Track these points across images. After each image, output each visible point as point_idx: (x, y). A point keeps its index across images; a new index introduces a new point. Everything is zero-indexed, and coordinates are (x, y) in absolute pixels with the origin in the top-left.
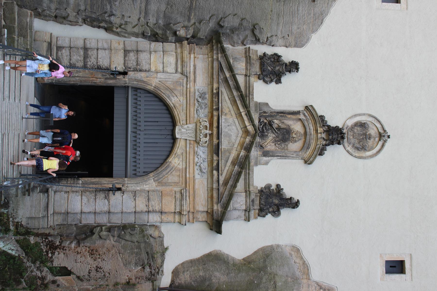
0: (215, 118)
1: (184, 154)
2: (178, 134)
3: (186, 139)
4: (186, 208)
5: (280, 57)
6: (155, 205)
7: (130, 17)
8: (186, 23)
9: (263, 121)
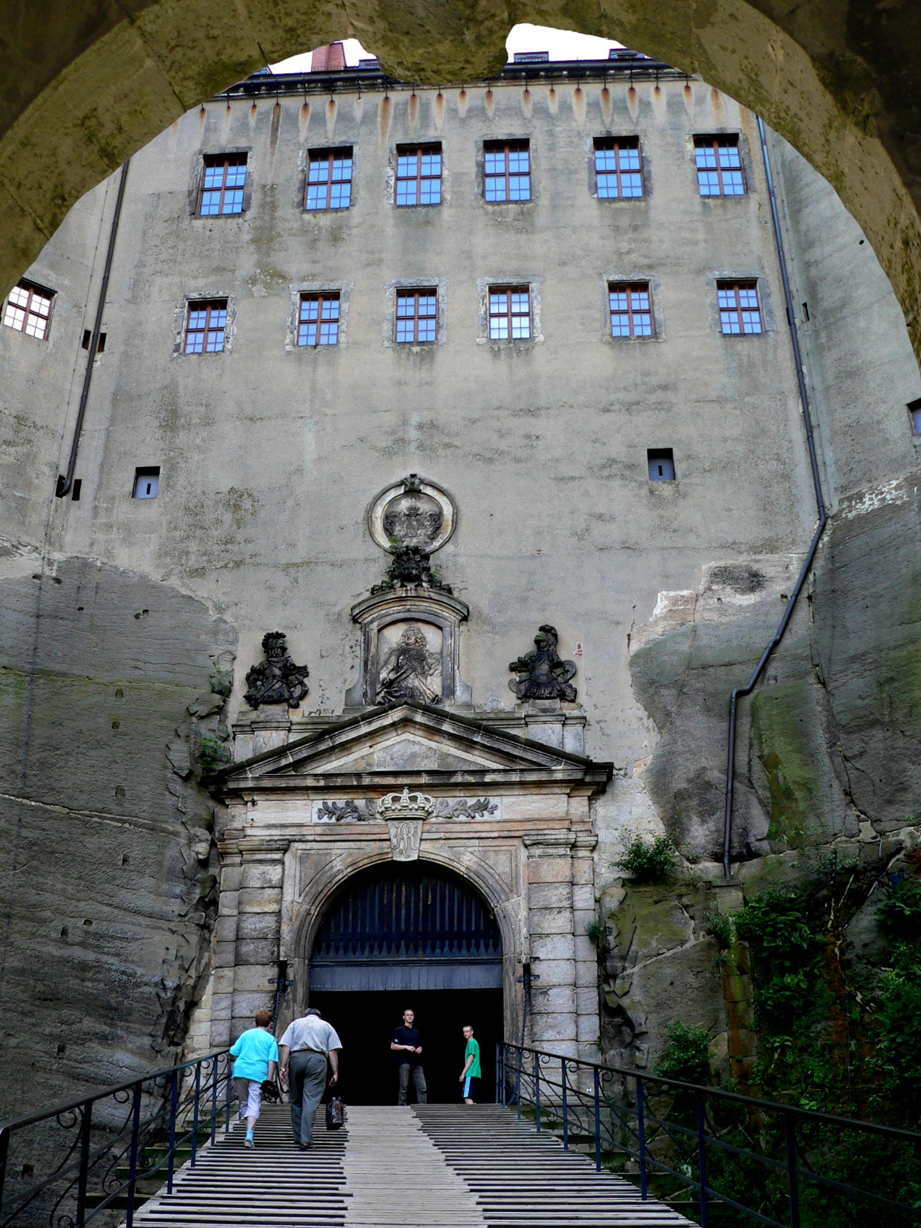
0: (378, 780)
1: (451, 842)
2: (409, 856)
3: (421, 840)
4: (562, 835)
5: (253, 670)
6: (556, 896)
7: (167, 949)
8: (183, 841)
9: (383, 698)
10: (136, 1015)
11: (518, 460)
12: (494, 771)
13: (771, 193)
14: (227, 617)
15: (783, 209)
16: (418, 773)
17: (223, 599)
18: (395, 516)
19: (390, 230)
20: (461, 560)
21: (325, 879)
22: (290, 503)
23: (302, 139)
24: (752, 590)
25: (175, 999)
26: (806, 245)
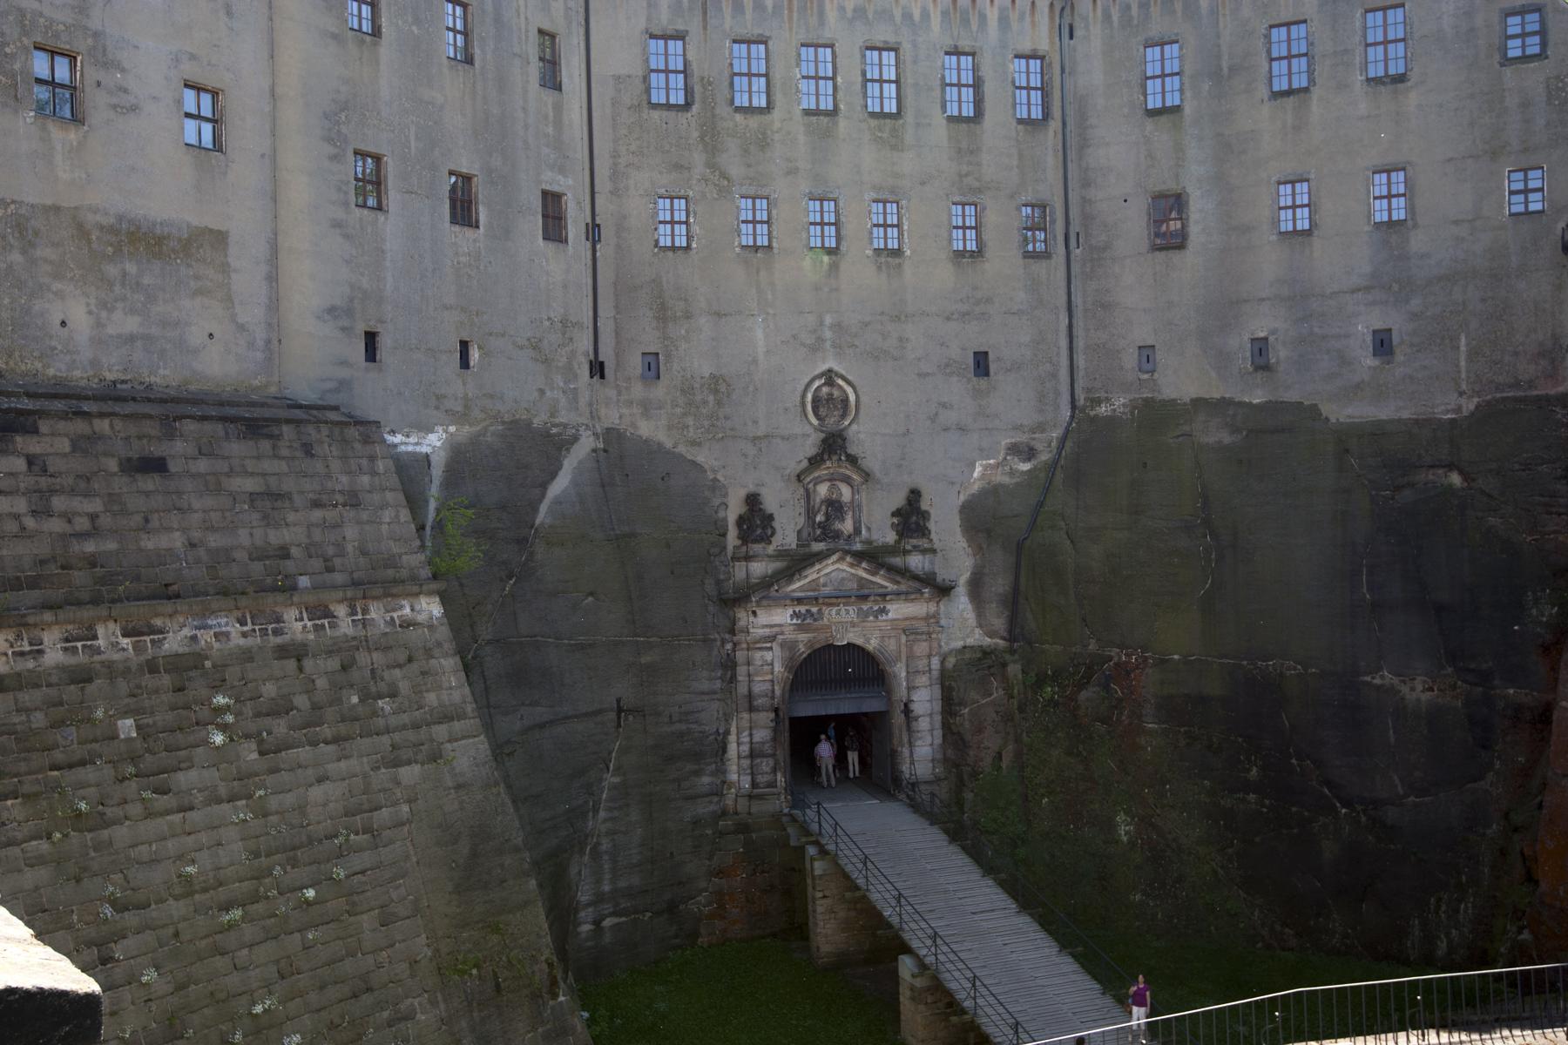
8: (719, 643)
13: (1064, 124)
15: (1073, 141)
17: (716, 463)
19: (802, 138)
20: (862, 436)
22: (751, 389)
23: (727, 26)
24: (1029, 460)
26: (1086, 184)
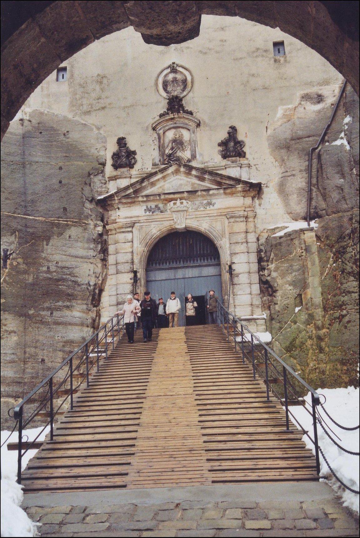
1: (198, 219)
4: (242, 213)
5: (114, 154)
6: (240, 238)
8: (92, 227)
10: (79, 297)
11: (217, 52)
12: (213, 189)
14: (102, 132)
16: (183, 192)
18: (167, 82)
21: (149, 237)
24: (319, 102)
25: (94, 289)
